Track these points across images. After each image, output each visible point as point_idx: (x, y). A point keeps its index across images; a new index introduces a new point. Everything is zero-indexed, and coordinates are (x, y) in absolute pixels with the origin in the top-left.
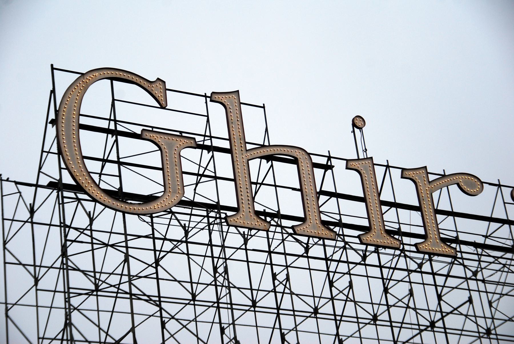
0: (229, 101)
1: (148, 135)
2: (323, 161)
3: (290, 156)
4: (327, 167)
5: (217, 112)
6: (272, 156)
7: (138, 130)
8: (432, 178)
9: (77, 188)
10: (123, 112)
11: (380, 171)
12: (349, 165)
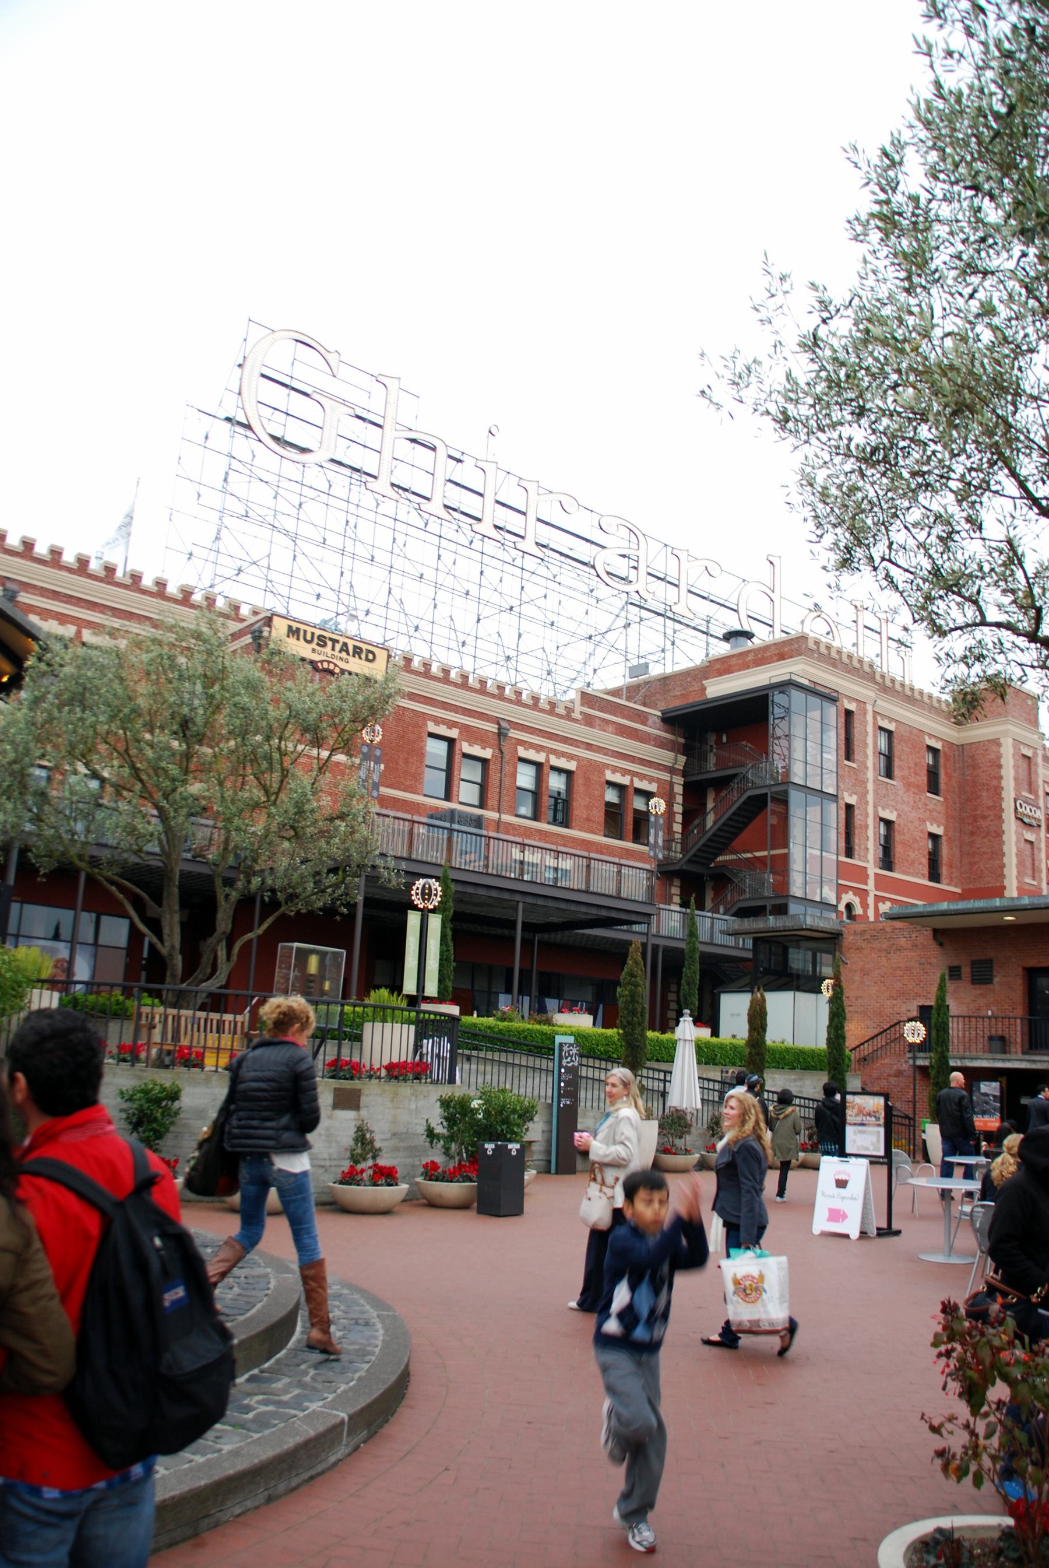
1: (315, 396)
2: (458, 455)
4: (459, 461)
7: (309, 390)
9: (248, 427)
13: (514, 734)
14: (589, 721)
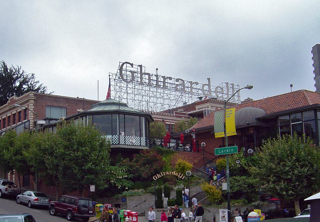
0: (141, 66)
2: (151, 75)
3: (148, 74)
5: (139, 68)
6: (145, 74)
8: (166, 77)
10: (128, 68)
11: (159, 76)
12: (155, 76)
13: (165, 120)
14: (176, 116)
